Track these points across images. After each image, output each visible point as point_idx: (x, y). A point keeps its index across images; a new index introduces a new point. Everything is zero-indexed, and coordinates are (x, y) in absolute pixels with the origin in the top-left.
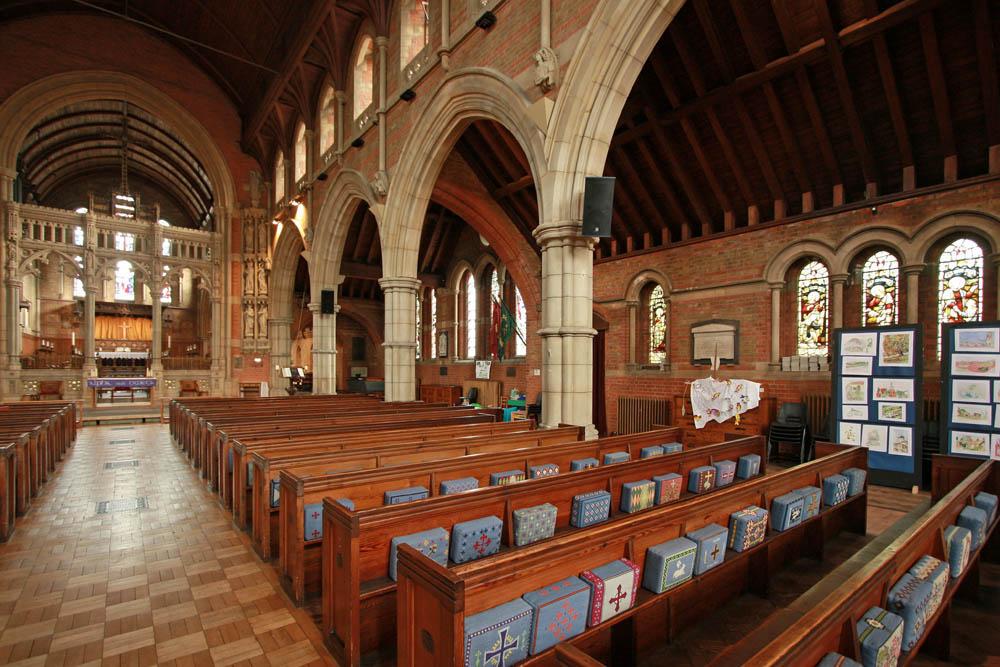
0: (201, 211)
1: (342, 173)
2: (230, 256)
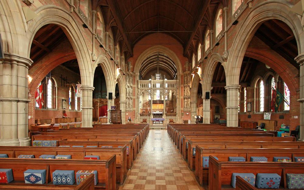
0: (174, 75)
1: (212, 55)
2: (181, 85)
